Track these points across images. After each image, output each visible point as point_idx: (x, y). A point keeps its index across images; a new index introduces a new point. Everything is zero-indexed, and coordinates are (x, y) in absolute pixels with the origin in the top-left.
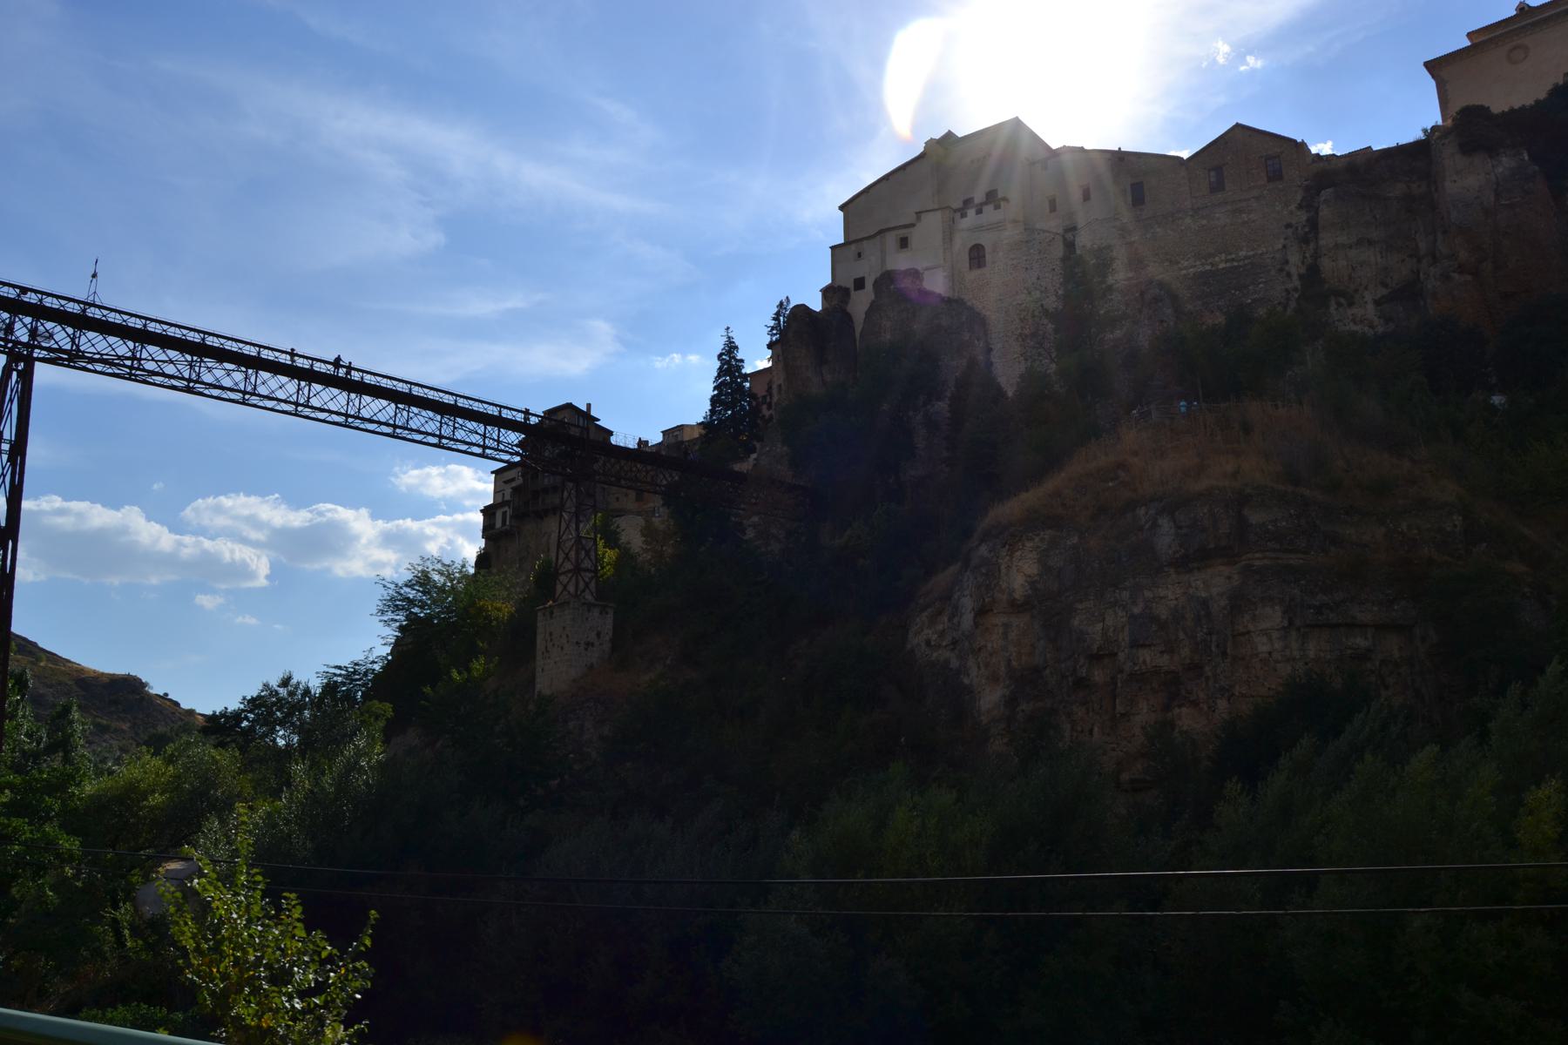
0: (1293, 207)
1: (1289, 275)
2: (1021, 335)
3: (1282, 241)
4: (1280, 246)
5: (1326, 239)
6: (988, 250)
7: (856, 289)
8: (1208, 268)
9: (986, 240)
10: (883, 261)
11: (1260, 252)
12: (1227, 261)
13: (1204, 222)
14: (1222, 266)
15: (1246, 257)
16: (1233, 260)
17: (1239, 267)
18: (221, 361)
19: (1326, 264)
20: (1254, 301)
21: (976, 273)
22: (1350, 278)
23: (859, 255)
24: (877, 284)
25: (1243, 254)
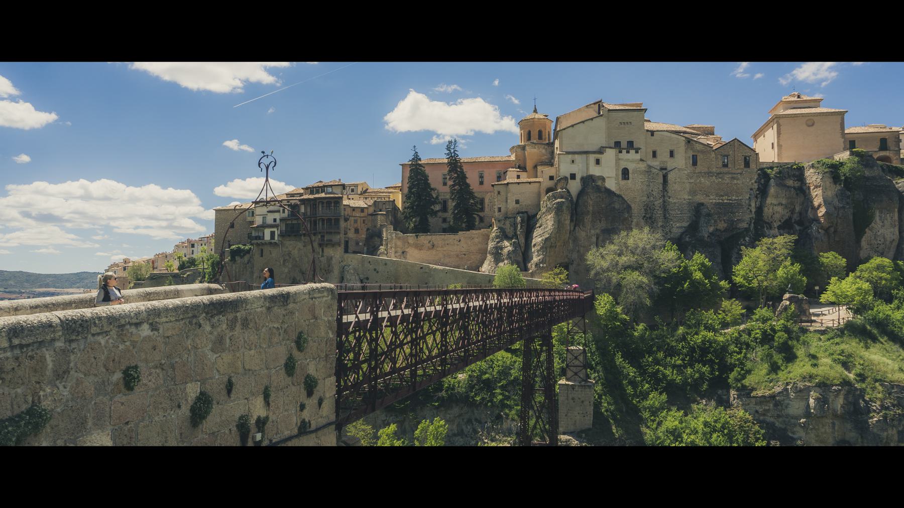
0: (753, 181)
1: (751, 211)
2: (645, 216)
3: (749, 195)
4: (748, 198)
5: (769, 200)
6: (630, 172)
7: (571, 179)
8: (721, 201)
9: (631, 167)
10: (587, 169)
11: (740, 198)
12: (728, 200)
13: (720, 180)
14: (725, 201)
15: (735, 200)
16: (730, 200)
17: (732, 203)
18: (893, 332)
19: (766, 209)
20: (738, 220)
21: (625, 181)
22: (772, 217)
23: (573, 161)
24: (582, 179)
25: (734, 198)
